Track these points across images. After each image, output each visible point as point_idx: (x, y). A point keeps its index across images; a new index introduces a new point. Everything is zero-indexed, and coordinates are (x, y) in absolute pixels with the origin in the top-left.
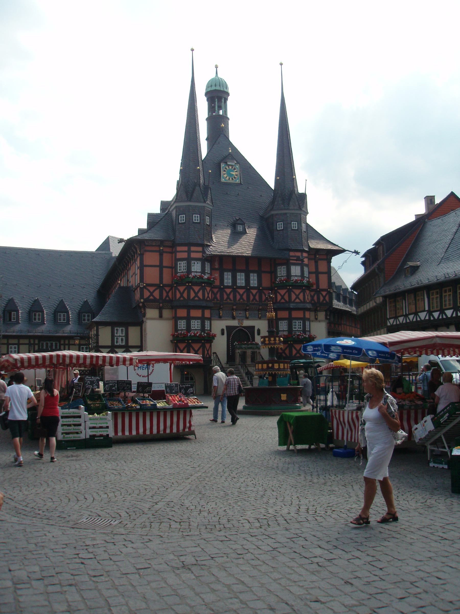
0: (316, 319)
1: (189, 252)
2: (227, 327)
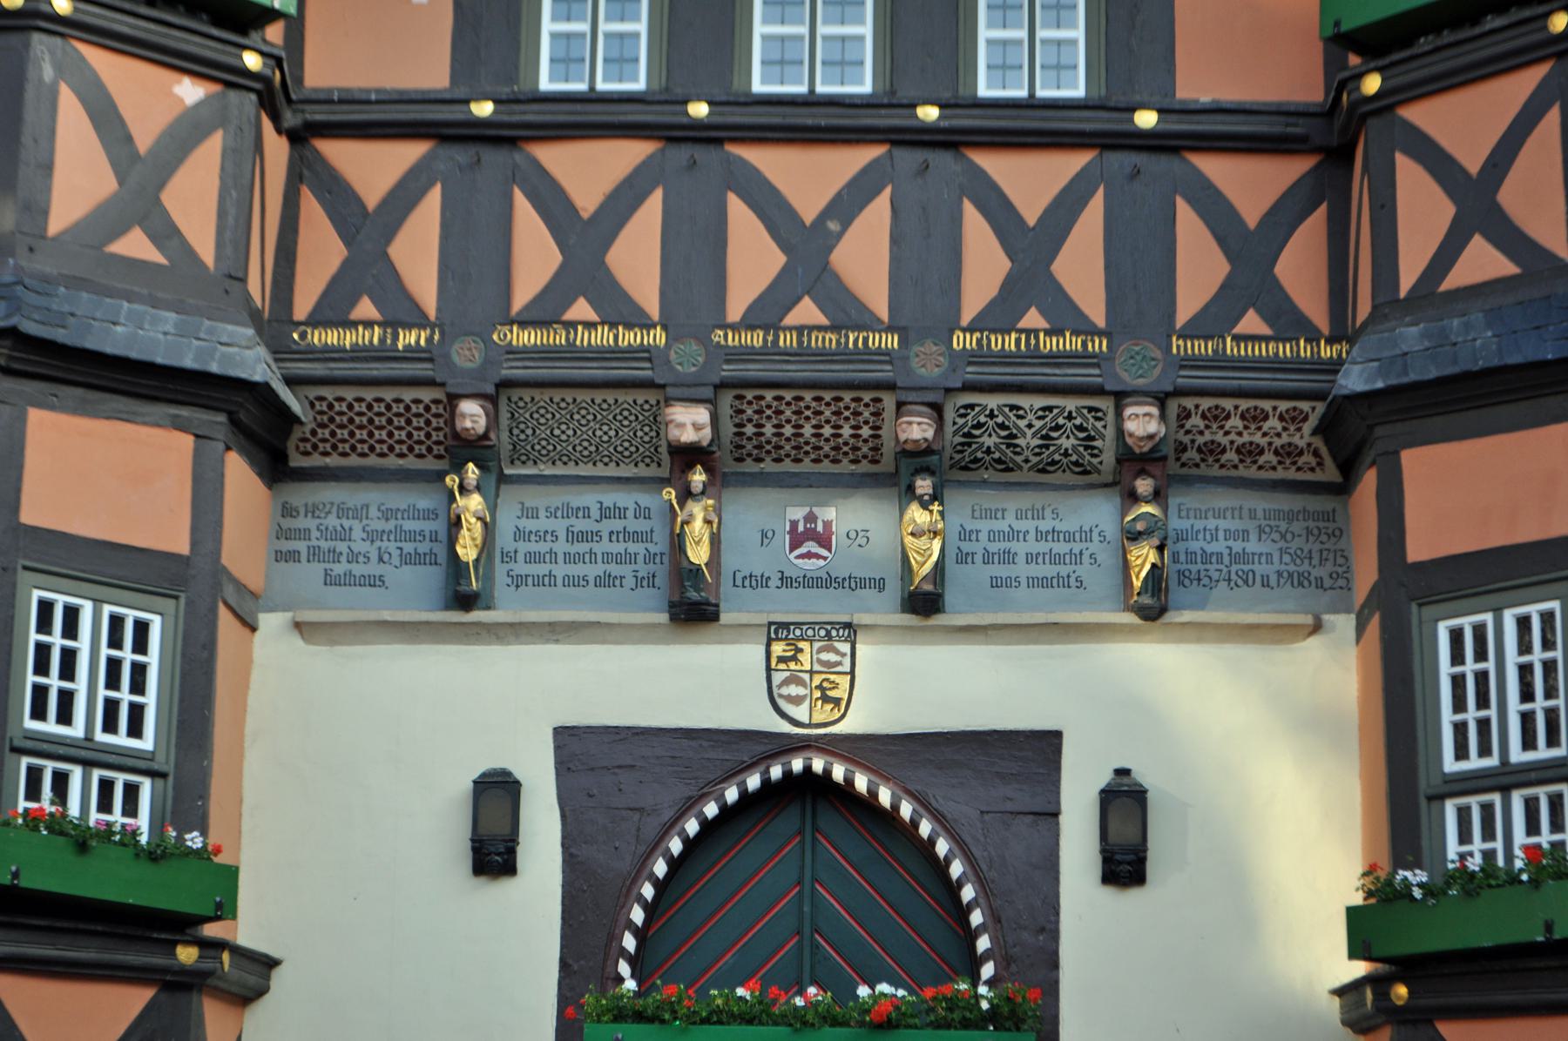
2: (577, 748)
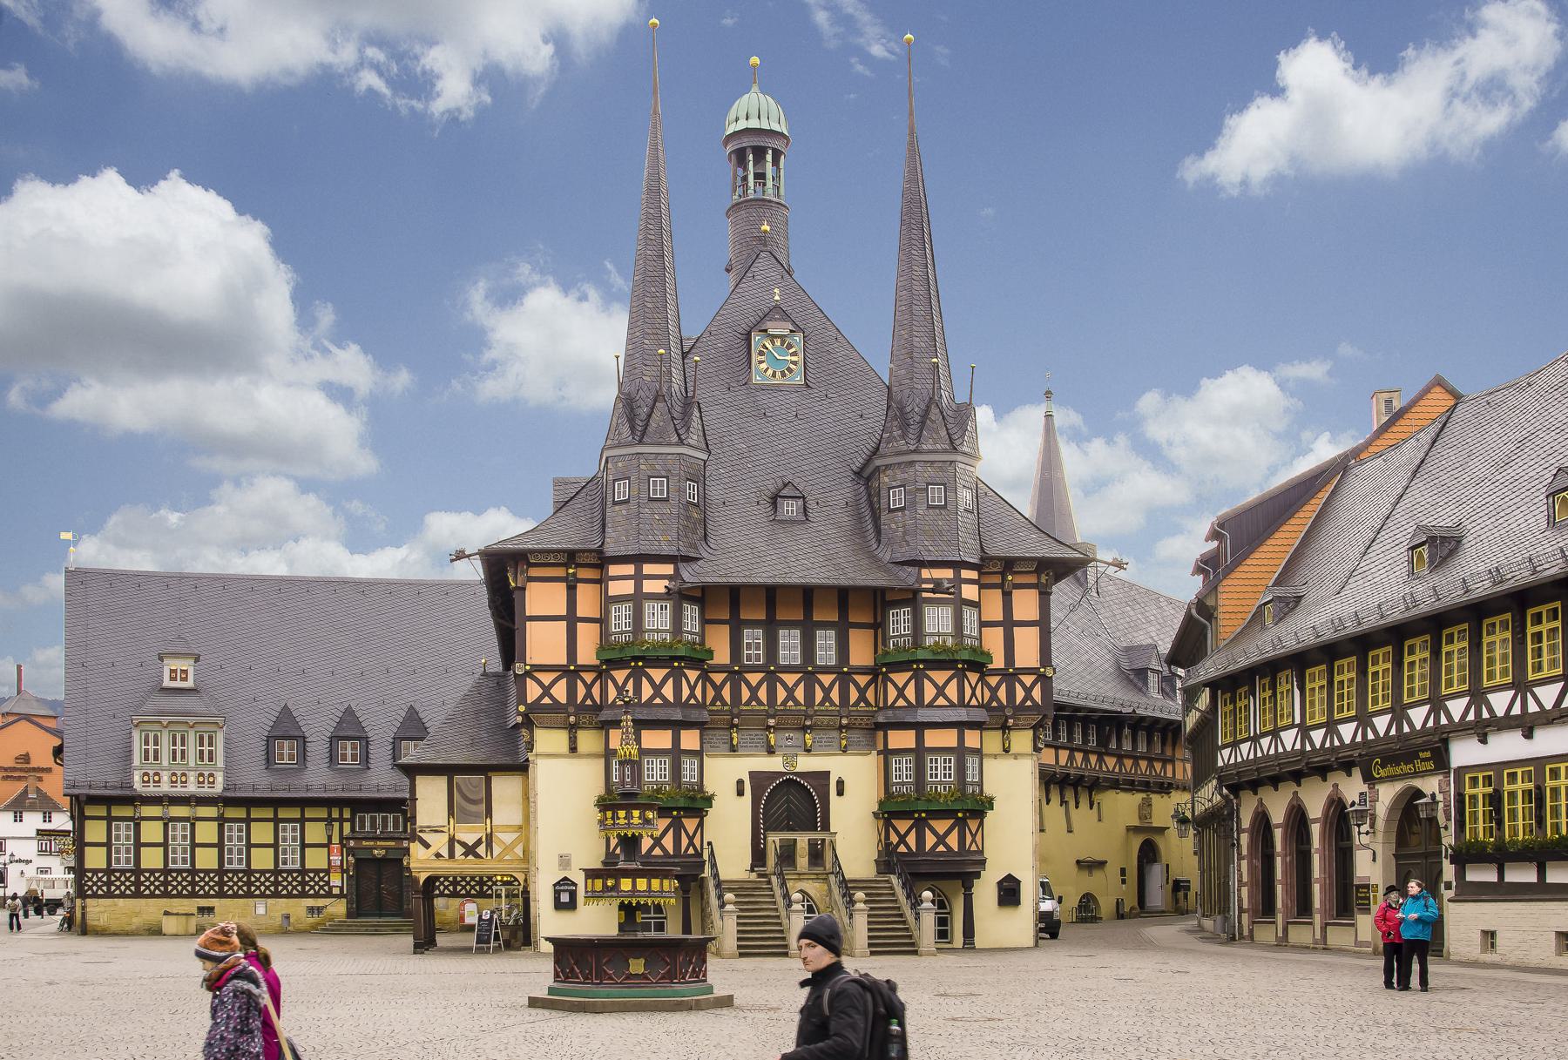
0: (1006, 751)
1: (639, 578)
